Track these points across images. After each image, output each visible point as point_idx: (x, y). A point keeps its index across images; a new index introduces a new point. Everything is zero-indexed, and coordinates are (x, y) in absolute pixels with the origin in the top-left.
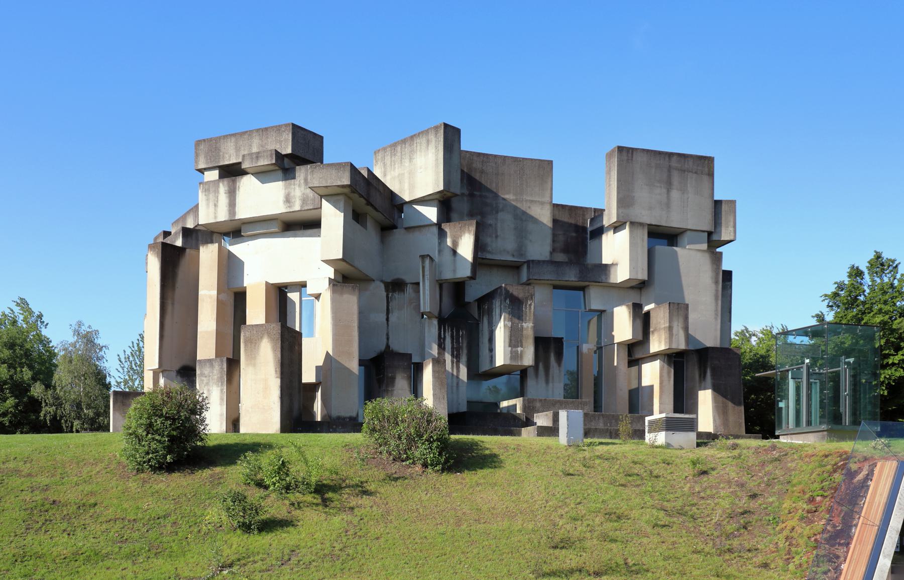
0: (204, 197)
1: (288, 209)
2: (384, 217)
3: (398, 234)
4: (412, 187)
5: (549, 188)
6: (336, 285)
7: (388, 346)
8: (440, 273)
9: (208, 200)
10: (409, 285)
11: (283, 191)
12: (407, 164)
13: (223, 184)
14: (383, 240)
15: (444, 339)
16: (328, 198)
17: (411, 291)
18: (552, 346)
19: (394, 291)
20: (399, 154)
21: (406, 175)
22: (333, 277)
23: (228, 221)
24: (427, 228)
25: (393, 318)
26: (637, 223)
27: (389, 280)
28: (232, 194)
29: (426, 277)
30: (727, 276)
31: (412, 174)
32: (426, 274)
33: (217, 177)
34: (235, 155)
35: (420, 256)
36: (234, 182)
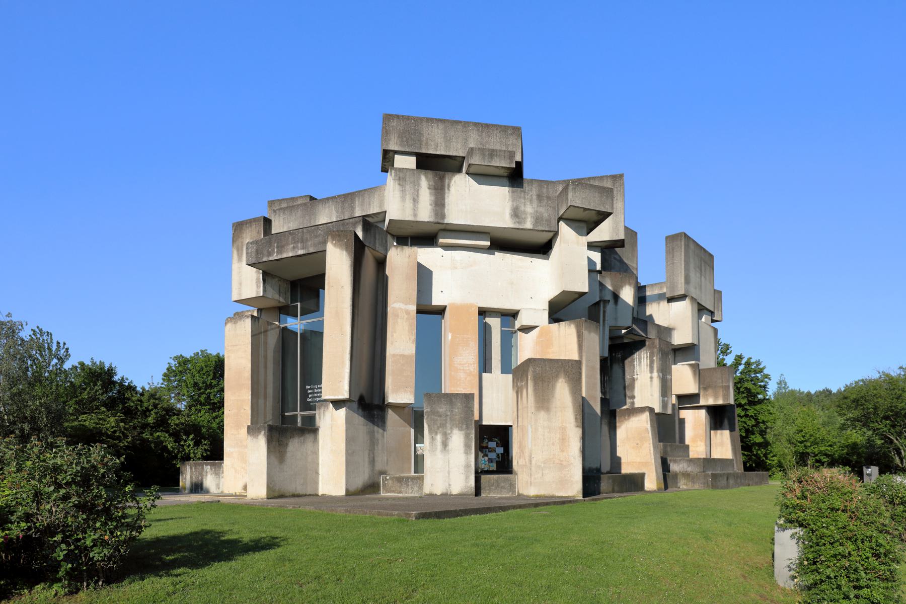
0: (397, 187)
1: (517, 224)
11: (510, 203)
13: (426, 177)
16: (569, 222)
23: (433, 222)
28: (439, 192)
29: (606, 322)
34: (443, 145)
36: (442, 179)
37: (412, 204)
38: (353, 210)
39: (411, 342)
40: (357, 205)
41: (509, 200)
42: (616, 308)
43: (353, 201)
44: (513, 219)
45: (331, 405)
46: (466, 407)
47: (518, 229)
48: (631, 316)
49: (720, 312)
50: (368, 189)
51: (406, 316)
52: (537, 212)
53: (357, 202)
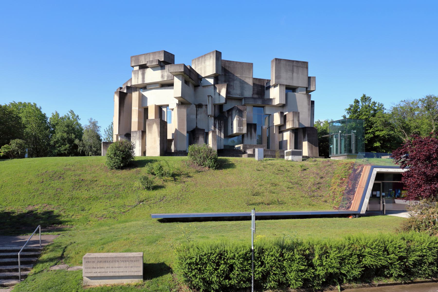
0: (134, 76)
3: (200, 88)
4: (205, 72)
5: (252, 72)
7: (197, 127)
8: (215, 101)
9: (135, 77)
11: (161, 74)
13: (140, 71)
14: (195, 90)
16: (176, 76)
17: (205, 108)
18: (253, 126)
19: (199, 108)
20: (200, 61)
21: (203, 68)
22: (178, 103)
25: (198, 117)
27: (197, 104)
28: (143, 74)
30: (313, 102)
31: (205, 67)
33: (138, 69)
36: (144, 70)
49: (314, 86)
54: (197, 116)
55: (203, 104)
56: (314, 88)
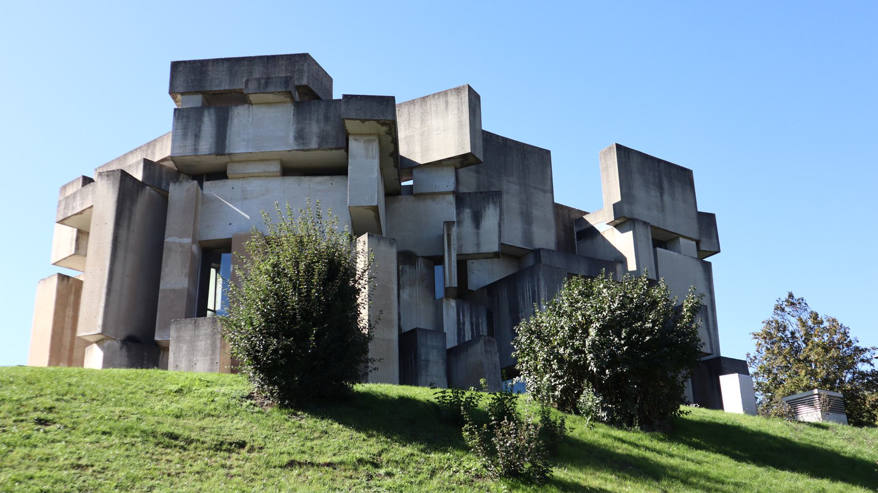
1: (302, 146)
2: (397, 177)
4: (425, 150)
6: (372, 236)
10: (420, 259)
11: (295, 126)
12: (418, 125)
15: (464, 324)
17: (422, 265)
19: (404, 263)
24: (442, 196)
25: (405, 295)
26: (641, 221)
29: (452, 246)
32: (452, 244)
35: (444, 222)
37: (193, 140)
38: (153, 156)
39: (184, 275)
40: (157, 150)
41: (293, 123)
42: (478, 234)
43: (155, 146)
44: (297, 141)
45: (95, 345)
46: (212, 331)
47: (303, 150)
48: (497, 240)
49: (715, 241)
50: (167, 133)
51: (180, 250)
52: (323, 131)
53: (157, 148)
54: (401, 290)
55: (419, 253)
56: (716, 246)
